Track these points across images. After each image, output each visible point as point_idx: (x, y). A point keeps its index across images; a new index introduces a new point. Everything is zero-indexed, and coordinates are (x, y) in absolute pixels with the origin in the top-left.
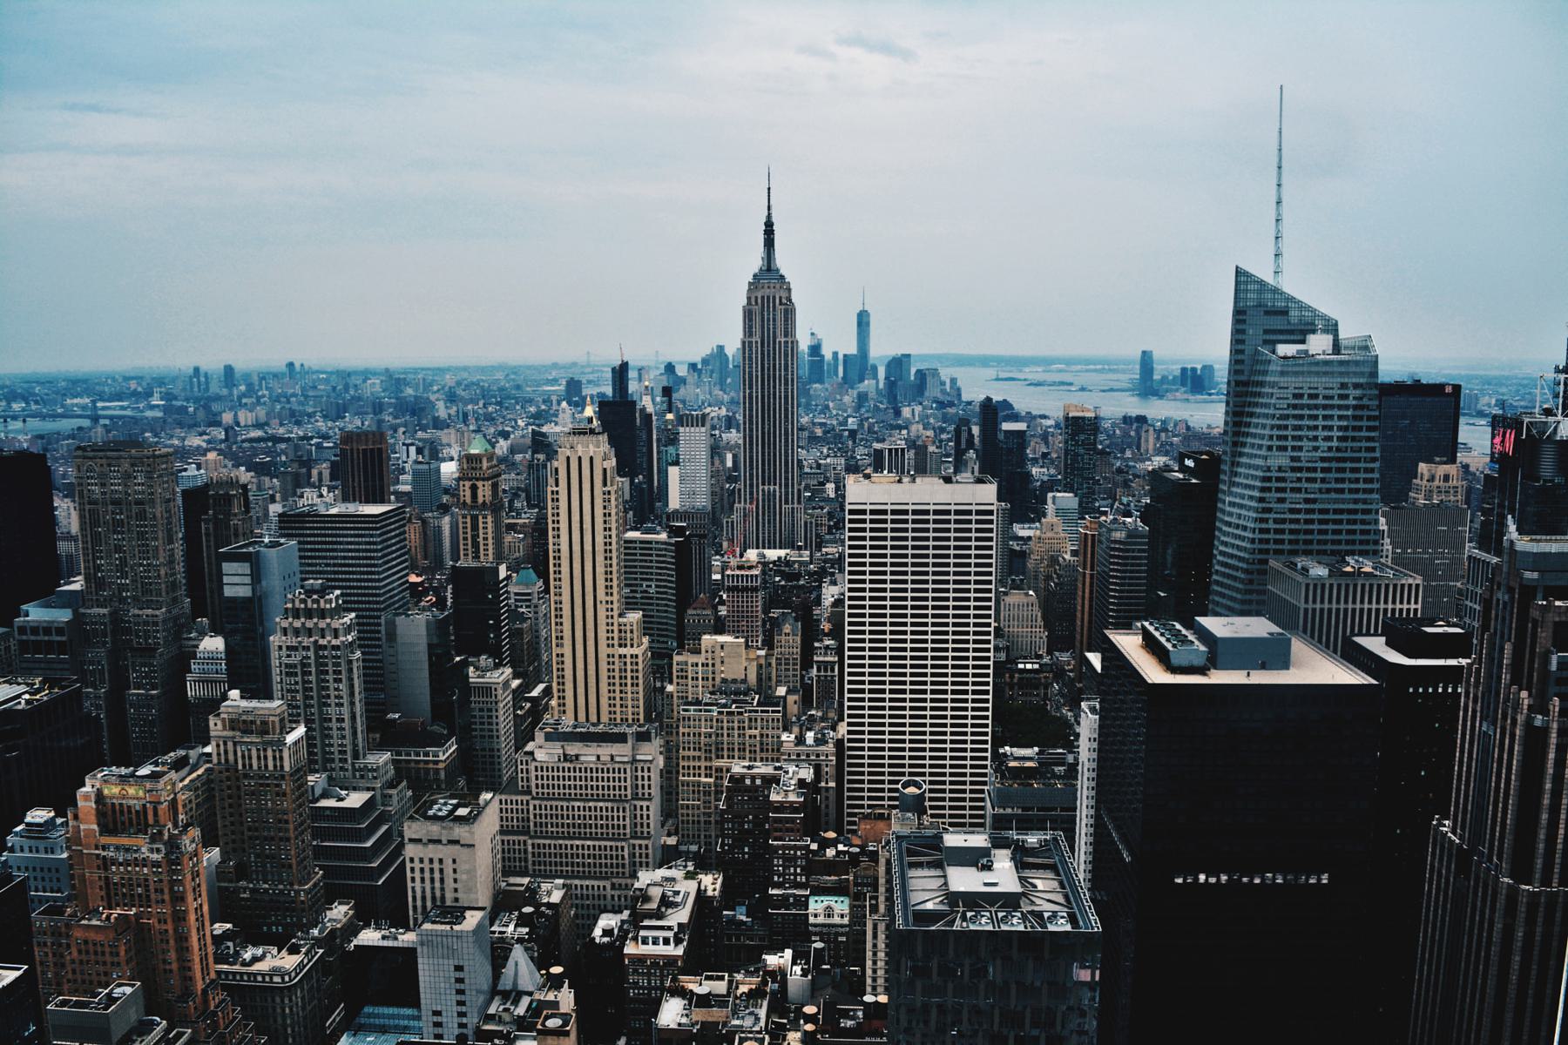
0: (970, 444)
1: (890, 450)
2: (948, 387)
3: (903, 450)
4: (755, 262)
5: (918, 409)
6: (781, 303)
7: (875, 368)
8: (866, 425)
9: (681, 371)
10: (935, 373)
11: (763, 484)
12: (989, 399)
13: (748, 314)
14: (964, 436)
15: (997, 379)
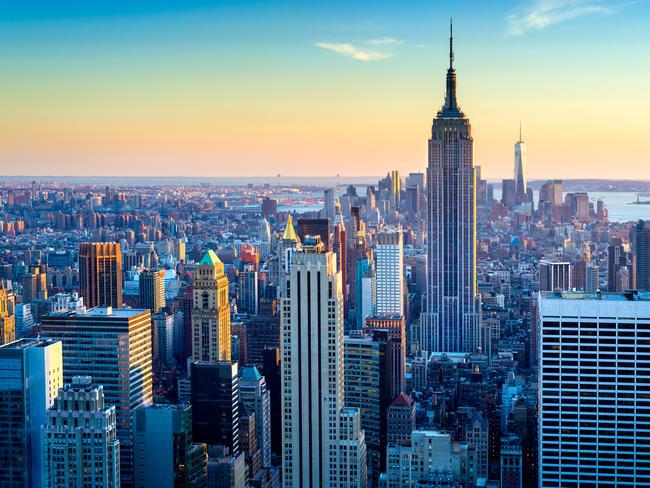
0: (623, 261)
1: (555, 266)
2: (595, 209)
3: (567, 266)
4: (439, 102)
5: (570, 229)
6: (461, 138)
7: (530, 191)
8: (526, 243)
9: (361, 192)
10: (584, 196)
11: (446, 295)
12: (641, 222)
13: (432, 145)
14: (617, 255)
15: (638, 203)
